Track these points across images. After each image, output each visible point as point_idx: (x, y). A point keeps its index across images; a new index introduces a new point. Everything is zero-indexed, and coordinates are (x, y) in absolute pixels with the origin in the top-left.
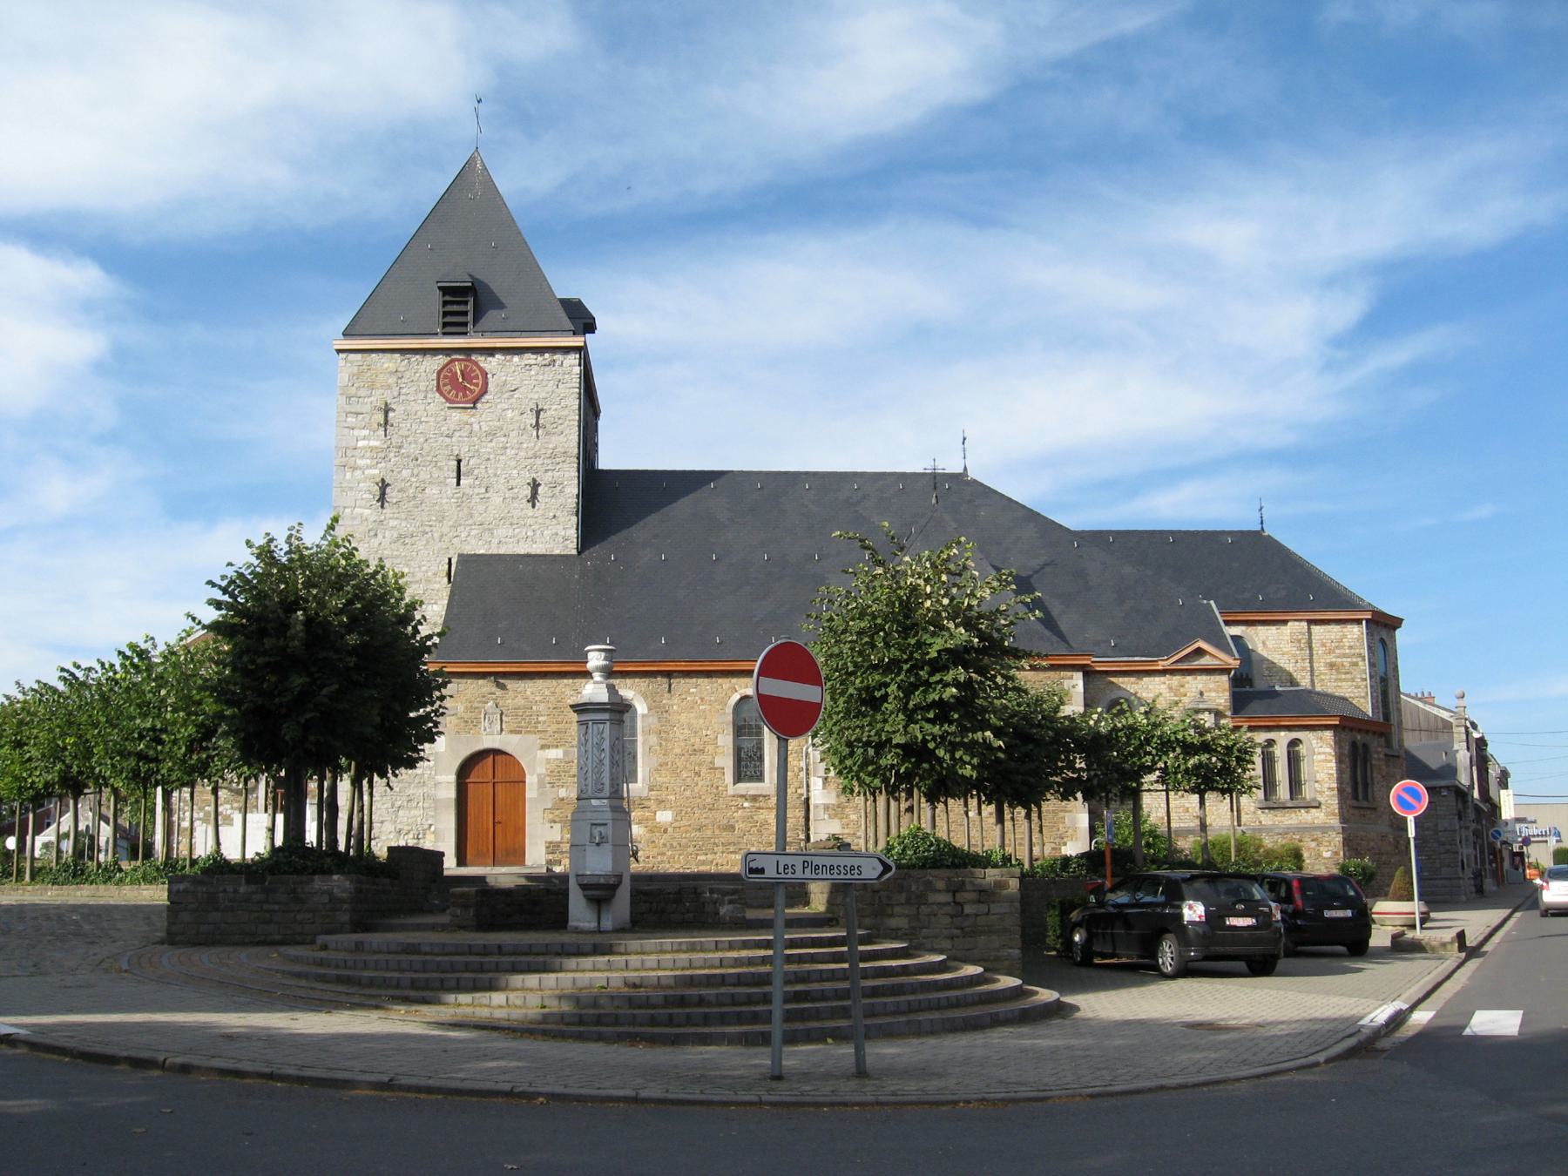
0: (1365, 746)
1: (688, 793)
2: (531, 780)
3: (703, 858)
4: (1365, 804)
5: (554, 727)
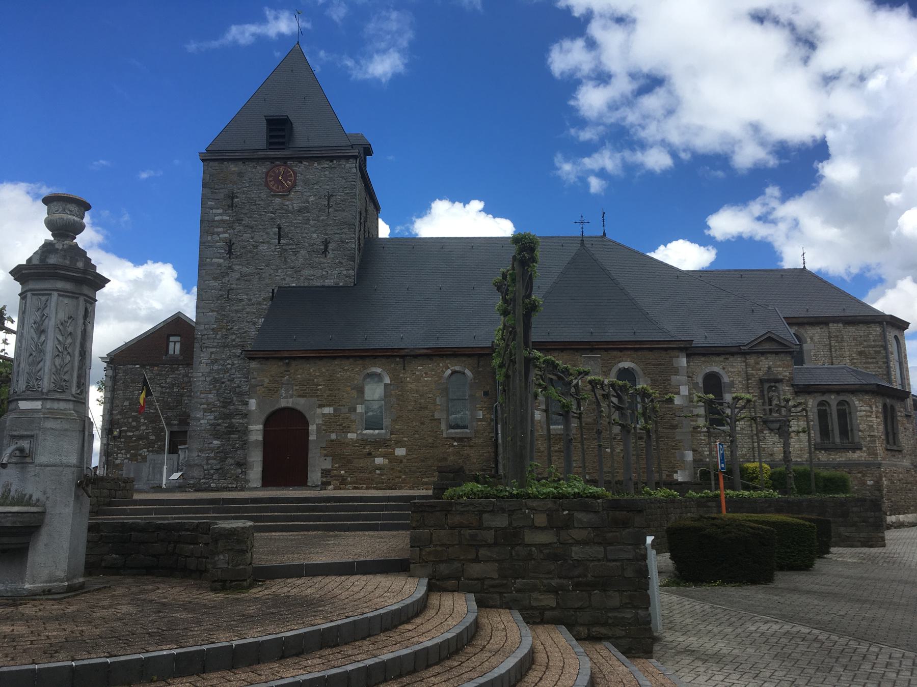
0: (892, 406)
1: (417, 436)
2: (312, 428)
3: (426, 480)
4: (895, 448)
5: (328, 392)
